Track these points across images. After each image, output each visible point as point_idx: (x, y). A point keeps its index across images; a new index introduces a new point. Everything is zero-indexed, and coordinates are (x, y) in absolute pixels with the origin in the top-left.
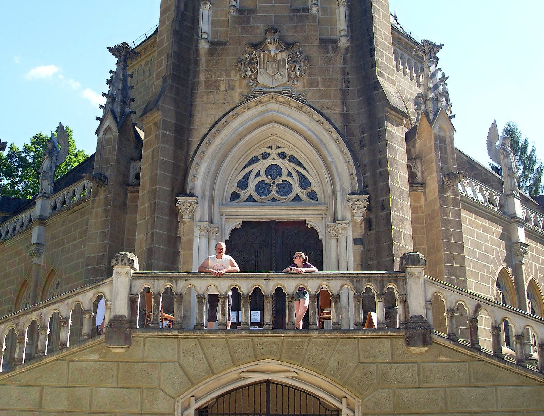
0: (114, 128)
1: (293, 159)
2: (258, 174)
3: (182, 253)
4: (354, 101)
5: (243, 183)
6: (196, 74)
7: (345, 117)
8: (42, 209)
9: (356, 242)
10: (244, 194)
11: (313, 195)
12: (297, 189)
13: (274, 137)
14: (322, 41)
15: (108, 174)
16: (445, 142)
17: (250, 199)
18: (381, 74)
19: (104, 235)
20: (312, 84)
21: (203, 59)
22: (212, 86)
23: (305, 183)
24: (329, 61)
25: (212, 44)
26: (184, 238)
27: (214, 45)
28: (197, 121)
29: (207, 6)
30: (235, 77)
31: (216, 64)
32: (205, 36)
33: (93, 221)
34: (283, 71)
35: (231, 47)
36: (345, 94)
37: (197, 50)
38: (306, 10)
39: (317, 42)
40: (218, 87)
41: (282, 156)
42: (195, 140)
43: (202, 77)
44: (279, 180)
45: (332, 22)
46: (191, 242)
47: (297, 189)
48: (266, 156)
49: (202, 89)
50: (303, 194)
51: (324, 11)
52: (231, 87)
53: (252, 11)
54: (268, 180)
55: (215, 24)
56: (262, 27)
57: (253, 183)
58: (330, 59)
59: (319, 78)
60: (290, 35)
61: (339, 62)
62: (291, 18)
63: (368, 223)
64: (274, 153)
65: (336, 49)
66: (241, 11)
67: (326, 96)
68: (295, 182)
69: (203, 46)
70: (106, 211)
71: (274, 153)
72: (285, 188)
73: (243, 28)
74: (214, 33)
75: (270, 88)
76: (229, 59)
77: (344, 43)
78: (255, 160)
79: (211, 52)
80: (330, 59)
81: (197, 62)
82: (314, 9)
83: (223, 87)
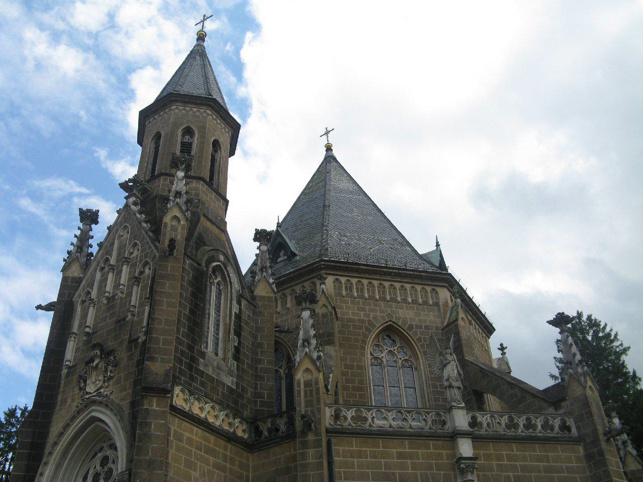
2: (95, 468)
13: (105, 433)
14: (130, 342)
16: (311, 385)
21: (63, 382)
22: (64, 401)
29: (73, 339)
30: (77, 391)
32: (68, 363)
34: (101, 378)
58: (132, 355)
69: (65, 371)
75: (91, 393)
79: (68, 375)
80: (132, 355)
81: (59, 387)
83: (68, 403)
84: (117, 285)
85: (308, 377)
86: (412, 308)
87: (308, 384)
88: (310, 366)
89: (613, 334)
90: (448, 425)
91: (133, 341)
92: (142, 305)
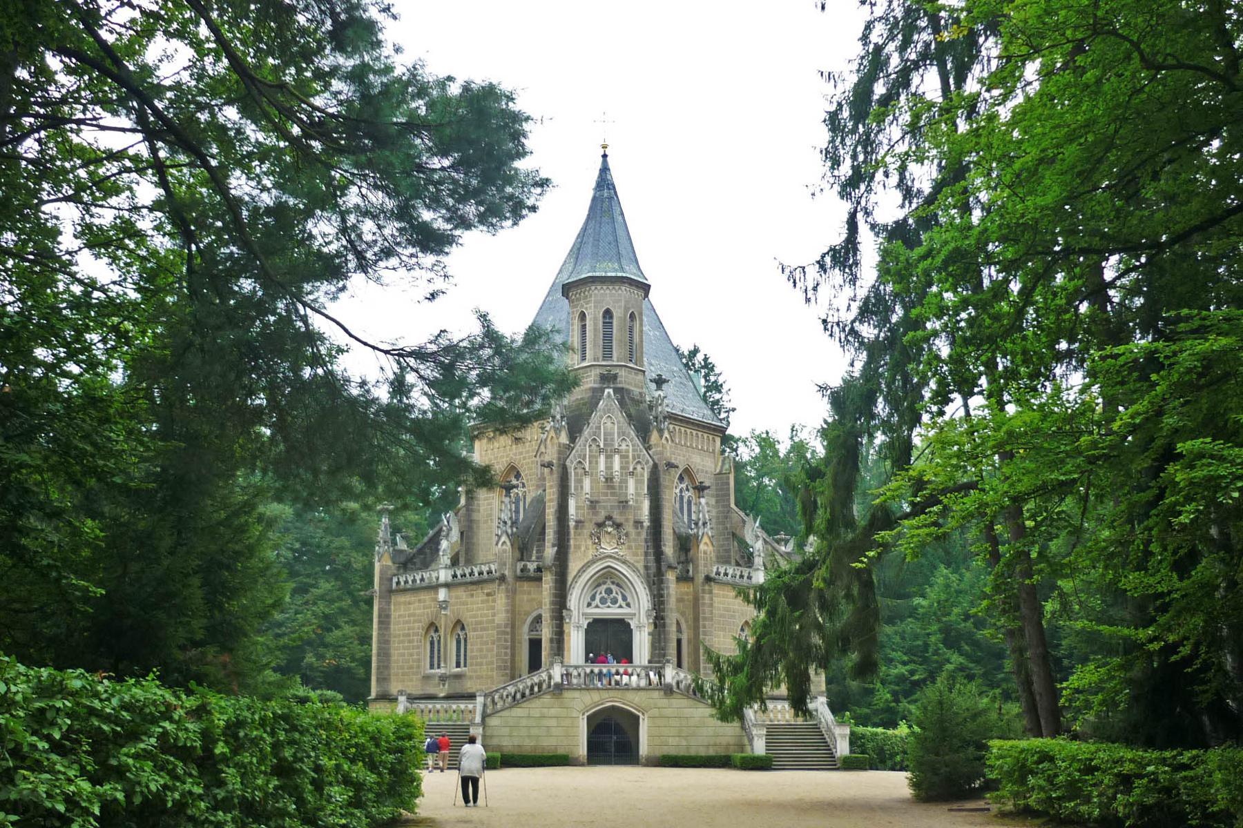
0: (509, 544)
1: (618, 585)
3: (566, 638)
4: (651, 558)
5: (593, 598)
6: (568, 540)
7: (646, 568)
8: (446, 577)
9: (649, 634)
10: (594, 604)
11: (628, 605)
12: (620, 601)
15: (506, 573)
17: (597, 607)
18: (665, 545)
19: (507, 611)
20: (630, 548)
21: (572, 531)
22: (578, 547)
23: (624, 598)
24: (639, 534)
25: (576, 522)
26: (566, 631)
27: (578, 522)
28: (570, 568)
30: (590, 542)
31: (579, 535)
33: (499, 602)
35: (586, 524)
36: (646, 554)
37: (568, 526)
38: (627, 502)
39: (631, 523)
40: (580, 548)
41: (613, 583)
42: (570, 579)
43: (572, 542)
44: (612, 596)
45: (639, 508)
46: (569, 633)
47: (620, 601)
48: (605, 583)
49: (572, 549)
50: (624, 605)
51: (637, 501)
52: (587, 548)
53: (597, 502)
54: (606, 596)
55: (577, 508)
56: (603, 514)
57: (598, 597)
59: (633, 544)
60: (618, 518)
61: (644, 535)
62: (619, 507)
63: (656, 626)
64: (609, 582)
65: (642, 527)
66: (592, 502)
67: (636, 554)
68: (620, 598)
69: (572, 524)
70: (508, 597)
71: (609, 582)
72: (615, 601)
73: (593, 514)
74: (577, 514)
76: (586, 532)
77: (647, 524)
78: (599, 585)
79: (576, 527)
81: (568, 533)
82: (631, 503)
83: (583, 549)
84: (609, 467)
85: (706, 548)
86: (700, 454)
87: (705, 553)
88: (708, 541)
89: (725, 388)
90: (753, 579)
91: (638, 523)
92: (638, 494)
